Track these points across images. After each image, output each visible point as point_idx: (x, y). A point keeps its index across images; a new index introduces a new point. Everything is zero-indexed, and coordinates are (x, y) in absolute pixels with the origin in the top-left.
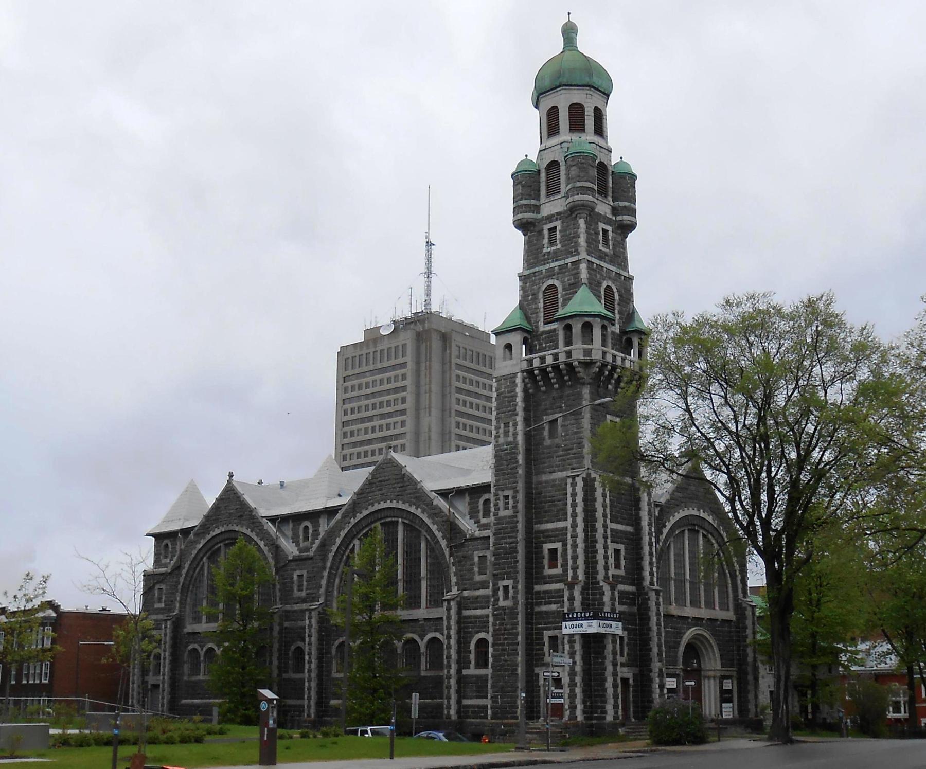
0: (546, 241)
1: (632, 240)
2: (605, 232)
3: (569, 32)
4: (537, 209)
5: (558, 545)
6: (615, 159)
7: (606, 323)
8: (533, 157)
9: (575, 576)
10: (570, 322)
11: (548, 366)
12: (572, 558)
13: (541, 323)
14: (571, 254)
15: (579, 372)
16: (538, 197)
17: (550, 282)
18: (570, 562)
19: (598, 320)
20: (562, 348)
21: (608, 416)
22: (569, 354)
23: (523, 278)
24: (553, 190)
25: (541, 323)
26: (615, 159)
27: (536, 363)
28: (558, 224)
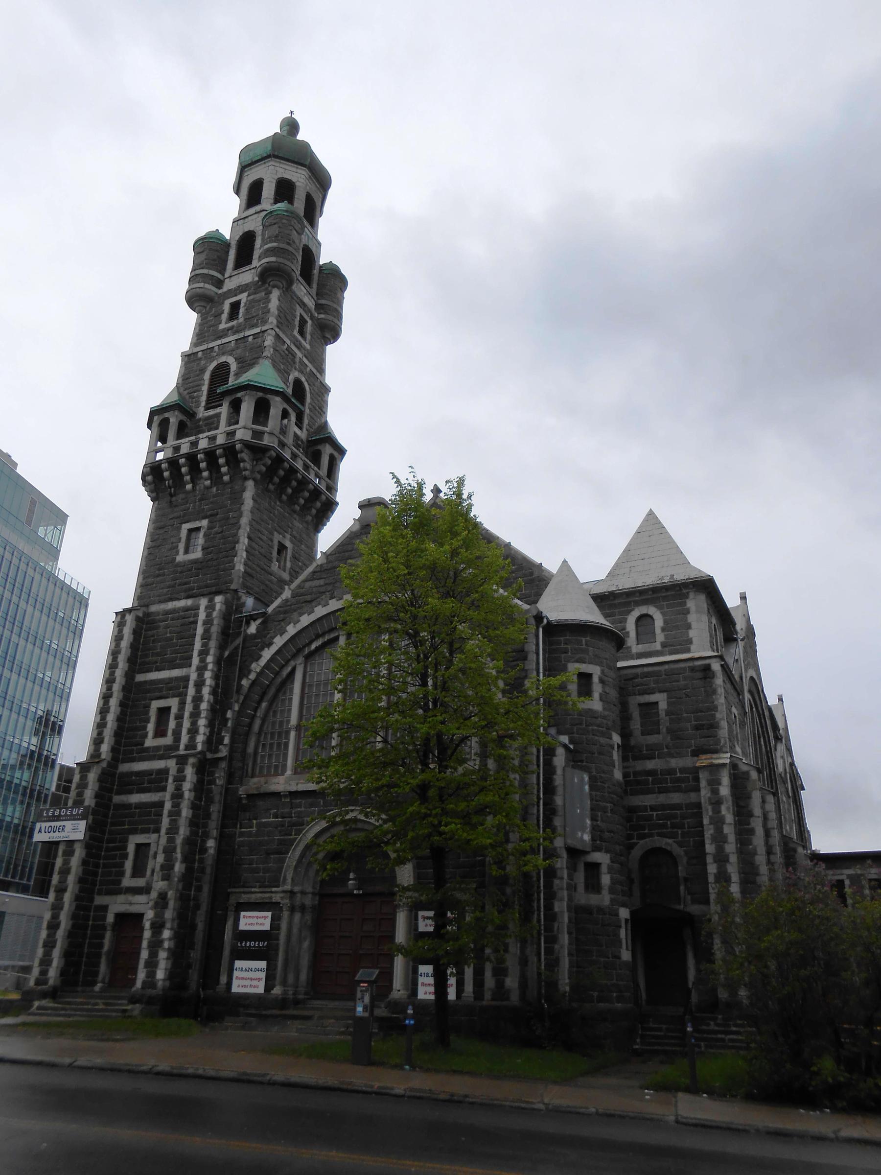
0: (225, 316)
1: (332, 351)
2: (303, 322)
3: (291, 126)
4: (219, 284)
5: (173, 703)
6: (324, 259)
7: (290, 410)
8: (227, 233)
9: (191, 745)
11: (199, 452)
12: (189, 731)
13: (201, 409)
15: (244, 461)
16: (222, 271)
17: (223, 359)
18: (186, 724)
19: (278, 399)
20: (223, 427)
21: (276, 533)
22: (231, 434)
23: (189, 359)
25: (201, 409)
26: (324, 259)
27: (185, 449)
28: (243, 297)
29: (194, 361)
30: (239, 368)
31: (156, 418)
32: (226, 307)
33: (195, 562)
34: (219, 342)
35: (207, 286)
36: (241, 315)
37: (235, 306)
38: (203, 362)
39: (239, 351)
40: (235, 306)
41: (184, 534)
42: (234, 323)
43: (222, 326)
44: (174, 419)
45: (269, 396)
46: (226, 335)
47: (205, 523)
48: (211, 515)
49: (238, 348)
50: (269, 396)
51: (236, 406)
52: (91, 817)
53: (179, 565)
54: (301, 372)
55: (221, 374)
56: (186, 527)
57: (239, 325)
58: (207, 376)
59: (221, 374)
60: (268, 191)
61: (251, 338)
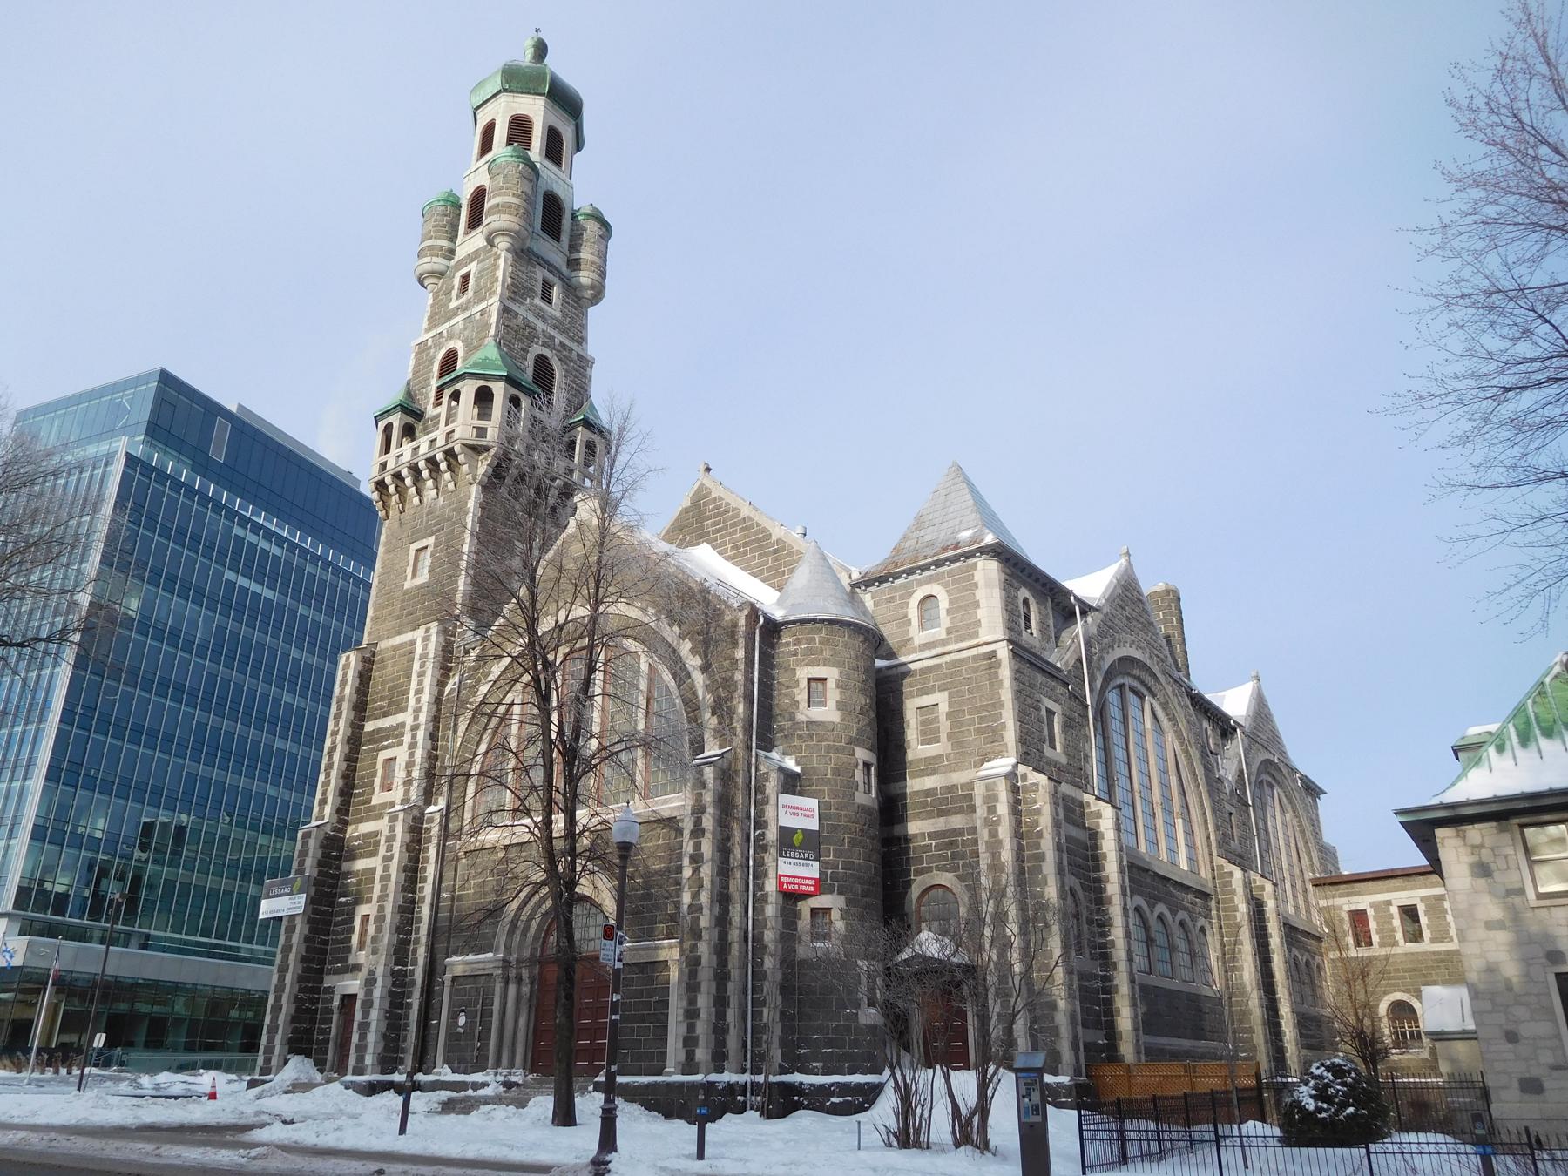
0: (455, 292)
3: (541, 50)
10: (457, 386)
14: (481, 301)
16: (453, 238)
24: (475, 221)
28: (472, 267)
29: (423, 351)
30: (466, 352)
31: (380, 423)
32: (457, 282)
33: (421, 587)
34: (447, 325)
35: (435, 259)
36: (470, 288)
37: (466, 278)
38: (432, 351)
39: (466, 333)
40: (466, 278)
41: (412, 554)
42: (464, 299)
43: (453, 305)
44: (396, 420)
45: (490, 384)
46: (456, 315)
47: (430, 541)
48: (438, 531)
49: (465, 329)
50: (490, 384)
51: (456, 396)
52: (313, 889)
53: (406, 592)
54: (544, 345)
55: (449, 362)
56: (415, 546)
57: (469, 301)
58: (436, 367)
59: (449, 362)
60: (500, 134)
61: (478, 316)
